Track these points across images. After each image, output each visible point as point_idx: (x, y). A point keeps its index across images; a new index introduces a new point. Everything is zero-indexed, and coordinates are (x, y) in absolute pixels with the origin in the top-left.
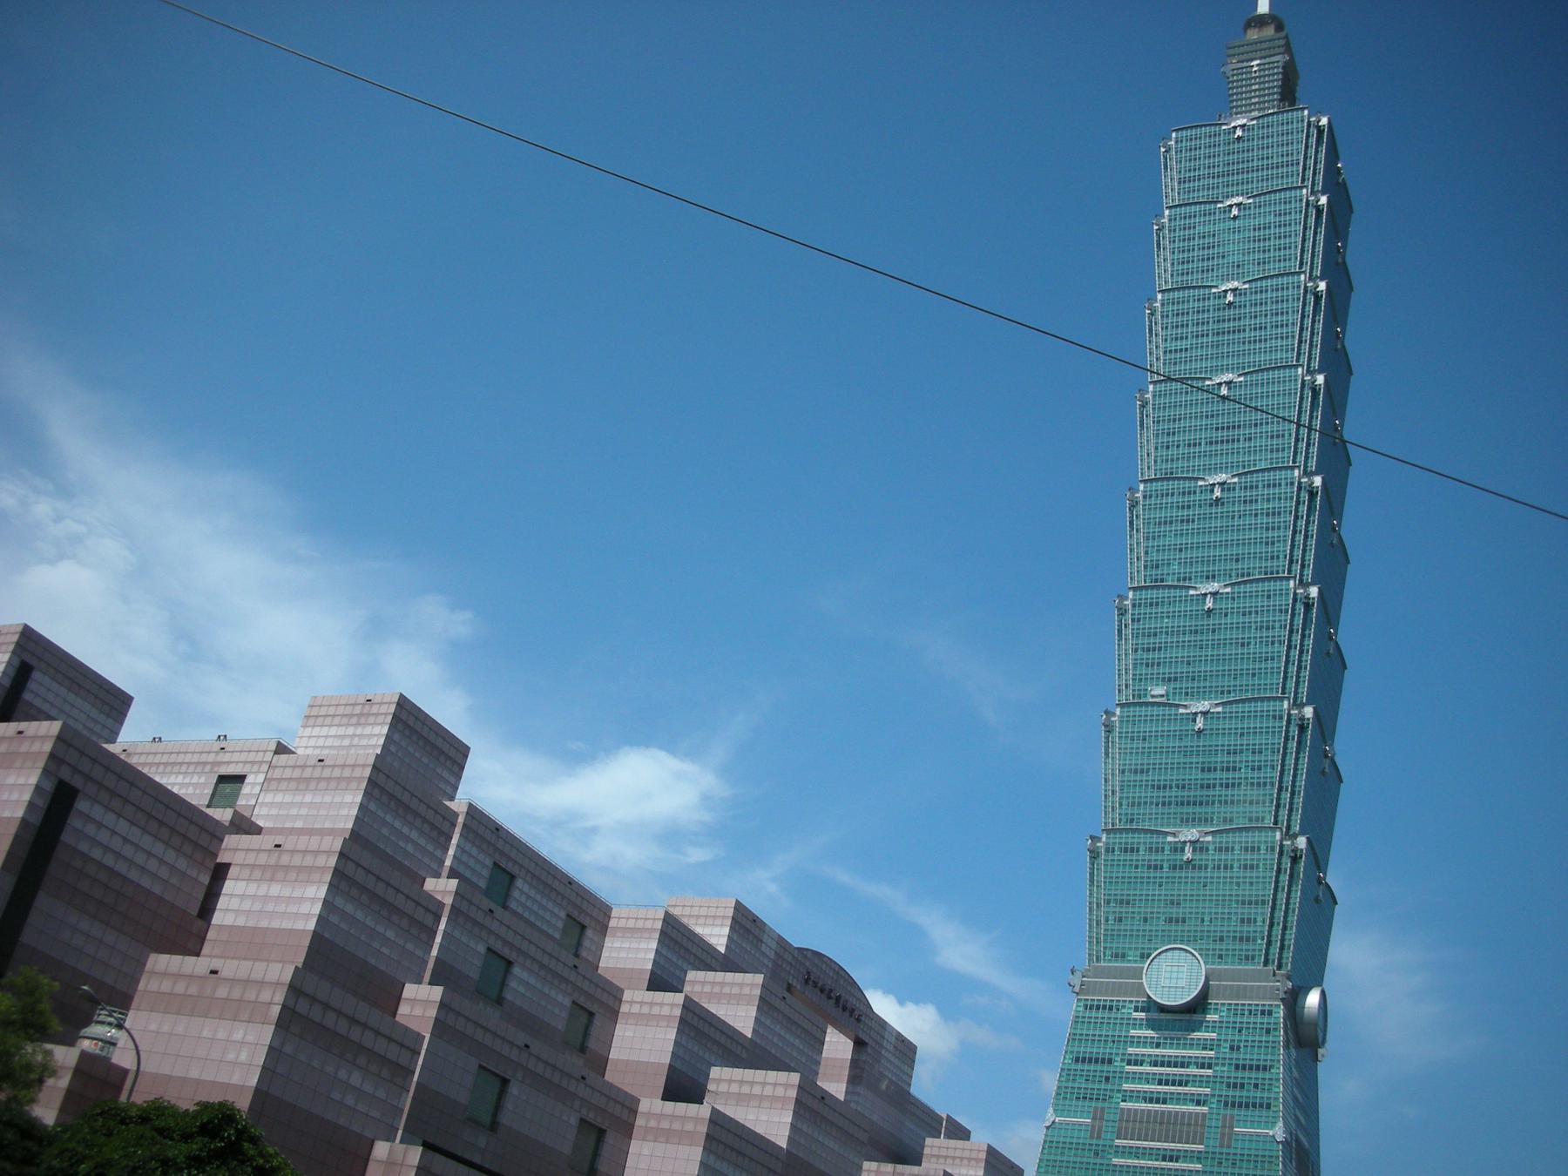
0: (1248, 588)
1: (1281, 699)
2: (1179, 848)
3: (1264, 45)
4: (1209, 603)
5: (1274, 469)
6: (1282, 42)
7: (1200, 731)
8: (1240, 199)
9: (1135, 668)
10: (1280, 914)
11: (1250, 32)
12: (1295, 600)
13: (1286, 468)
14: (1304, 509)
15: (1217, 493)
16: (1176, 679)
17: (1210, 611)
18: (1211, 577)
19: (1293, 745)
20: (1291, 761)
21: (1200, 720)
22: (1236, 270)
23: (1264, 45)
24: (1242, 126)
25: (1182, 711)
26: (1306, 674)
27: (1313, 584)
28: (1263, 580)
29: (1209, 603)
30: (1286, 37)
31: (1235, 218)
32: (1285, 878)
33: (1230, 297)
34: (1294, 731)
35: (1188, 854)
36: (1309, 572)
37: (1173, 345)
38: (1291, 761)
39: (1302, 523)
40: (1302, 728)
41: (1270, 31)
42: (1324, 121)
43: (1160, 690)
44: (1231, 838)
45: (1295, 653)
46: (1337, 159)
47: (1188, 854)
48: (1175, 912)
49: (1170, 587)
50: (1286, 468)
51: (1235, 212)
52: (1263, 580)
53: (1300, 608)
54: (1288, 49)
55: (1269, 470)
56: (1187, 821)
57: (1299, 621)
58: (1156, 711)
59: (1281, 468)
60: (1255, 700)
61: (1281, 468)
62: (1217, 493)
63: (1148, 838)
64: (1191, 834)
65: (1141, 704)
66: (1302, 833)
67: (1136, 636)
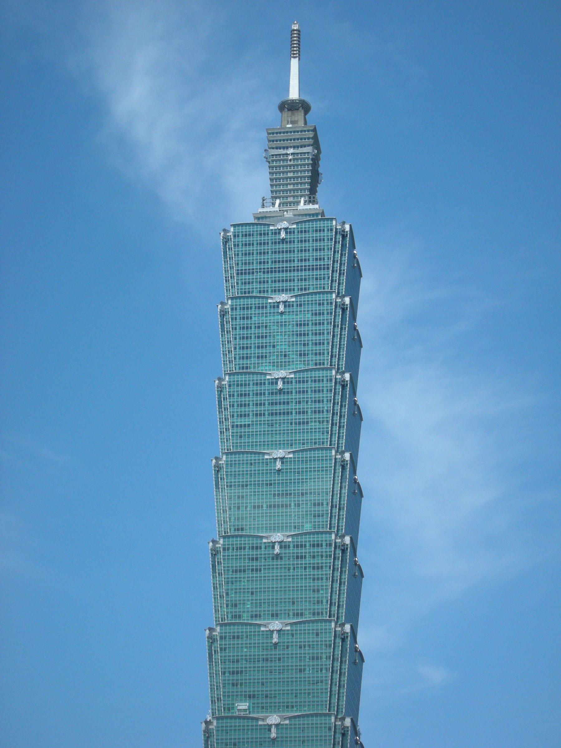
0: (303, 627)
1: (330, 715)
3: (297, 135)
5: (318, 533)
6: (311, 134)
7: (274, 740)
8: (284, 297)
9: (224, 687)
11: (286, 113)
12: (335, 637)
13: (326, 533)
14: (338, 563)
15: (277, 550)
16: (254, 696)
17: (276, 644)
18: (275, 616)
21: (273, 729)
23: (297, 135)
24: (286, 229)
25: (260, 723)
27: (347, 621)
28: (313, 622)
30: (315, 130)
31: (282, 313)
33: (280, 385)
34: (339, 737)
36: (343, 611)
37: (239, 421)
40: (344, 735)
41: (299, 116)
42: (347, 227)
43: (243, 706)
46: (354, 248)
49: (246, 624)
50: (326, 533)
51: (282, 308)
52: (313, 622)
53: (339, 641)
54: (316, 144)
55: (313, 533)
57: (338, 652)
59: (322, 533)
60: (312, 715)
61: (322, 533)
62: (277, 550)
65: (231, 718)
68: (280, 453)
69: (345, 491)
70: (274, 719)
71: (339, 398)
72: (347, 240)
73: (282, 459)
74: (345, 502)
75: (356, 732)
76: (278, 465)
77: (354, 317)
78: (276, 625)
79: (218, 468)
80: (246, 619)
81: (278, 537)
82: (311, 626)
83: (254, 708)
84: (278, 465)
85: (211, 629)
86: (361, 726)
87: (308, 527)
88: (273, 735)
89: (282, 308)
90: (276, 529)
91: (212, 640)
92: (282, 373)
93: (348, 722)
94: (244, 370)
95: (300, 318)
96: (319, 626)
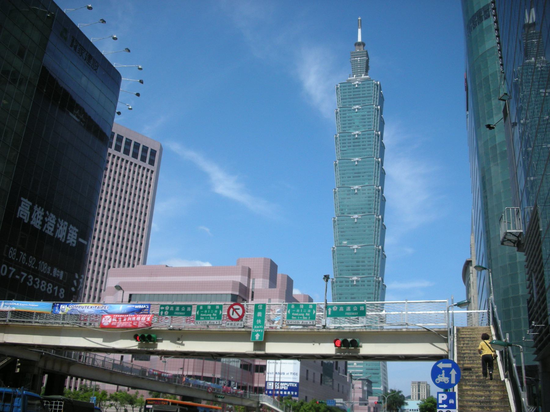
2: (353, 281)
4: (356, 221)
7: (355, 253)
8: (357, 107)
10: (376, 296)
15: (356, 191)
18: (355, 213)
19: (377, 256)
20: (377, 259)
22: (357, 128)
26: (379, 237)
29: (356, 221)
32: (377, 287)
33: (356, 136)
35: (355, 283)
36: (379, 211)
38: (377, 259)
39: (377, 199)
40: (379, 251)
43: (345, 242)
44: (364, 279)
45: (377, 233)
47: (355, 283)
48: (353, 296)
51: (356, 110)
53: (377, 222)
56: (354, 274)
57: (377, 225)
58: (345, 248)
62: (356, 191)
63: (346, 279)
64: (355, 278)
66: (380, 276)
67: (338, 228)
68: (357, 159)
69: (379, 171)
70: (355, 247)
71: (377, 140)
72: (379, 87)
73: (357, 161)
74: (379, 175)
75: (383, 251)
76: (356, 163)
77: (381, 113)
78: (356, 216)
79: (336, 165)
80: (346, 215)
81: (356, 187)
82: (368, 216)
83: (348, 243)
84: (356, 163)
85: (334, 218)
86: (385, 249)
87: (367, 184)
88: (355, 252)
89: (356, 110)
90: (355, 184)
91: (334, 221)
92: (357, 132)
93: (380, 247)
94: (344, 132)
95: (363, 113)
96: (370, 216)
